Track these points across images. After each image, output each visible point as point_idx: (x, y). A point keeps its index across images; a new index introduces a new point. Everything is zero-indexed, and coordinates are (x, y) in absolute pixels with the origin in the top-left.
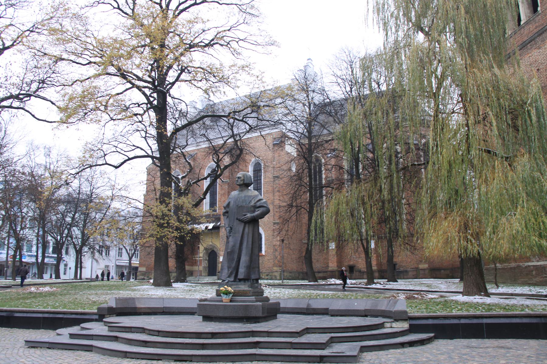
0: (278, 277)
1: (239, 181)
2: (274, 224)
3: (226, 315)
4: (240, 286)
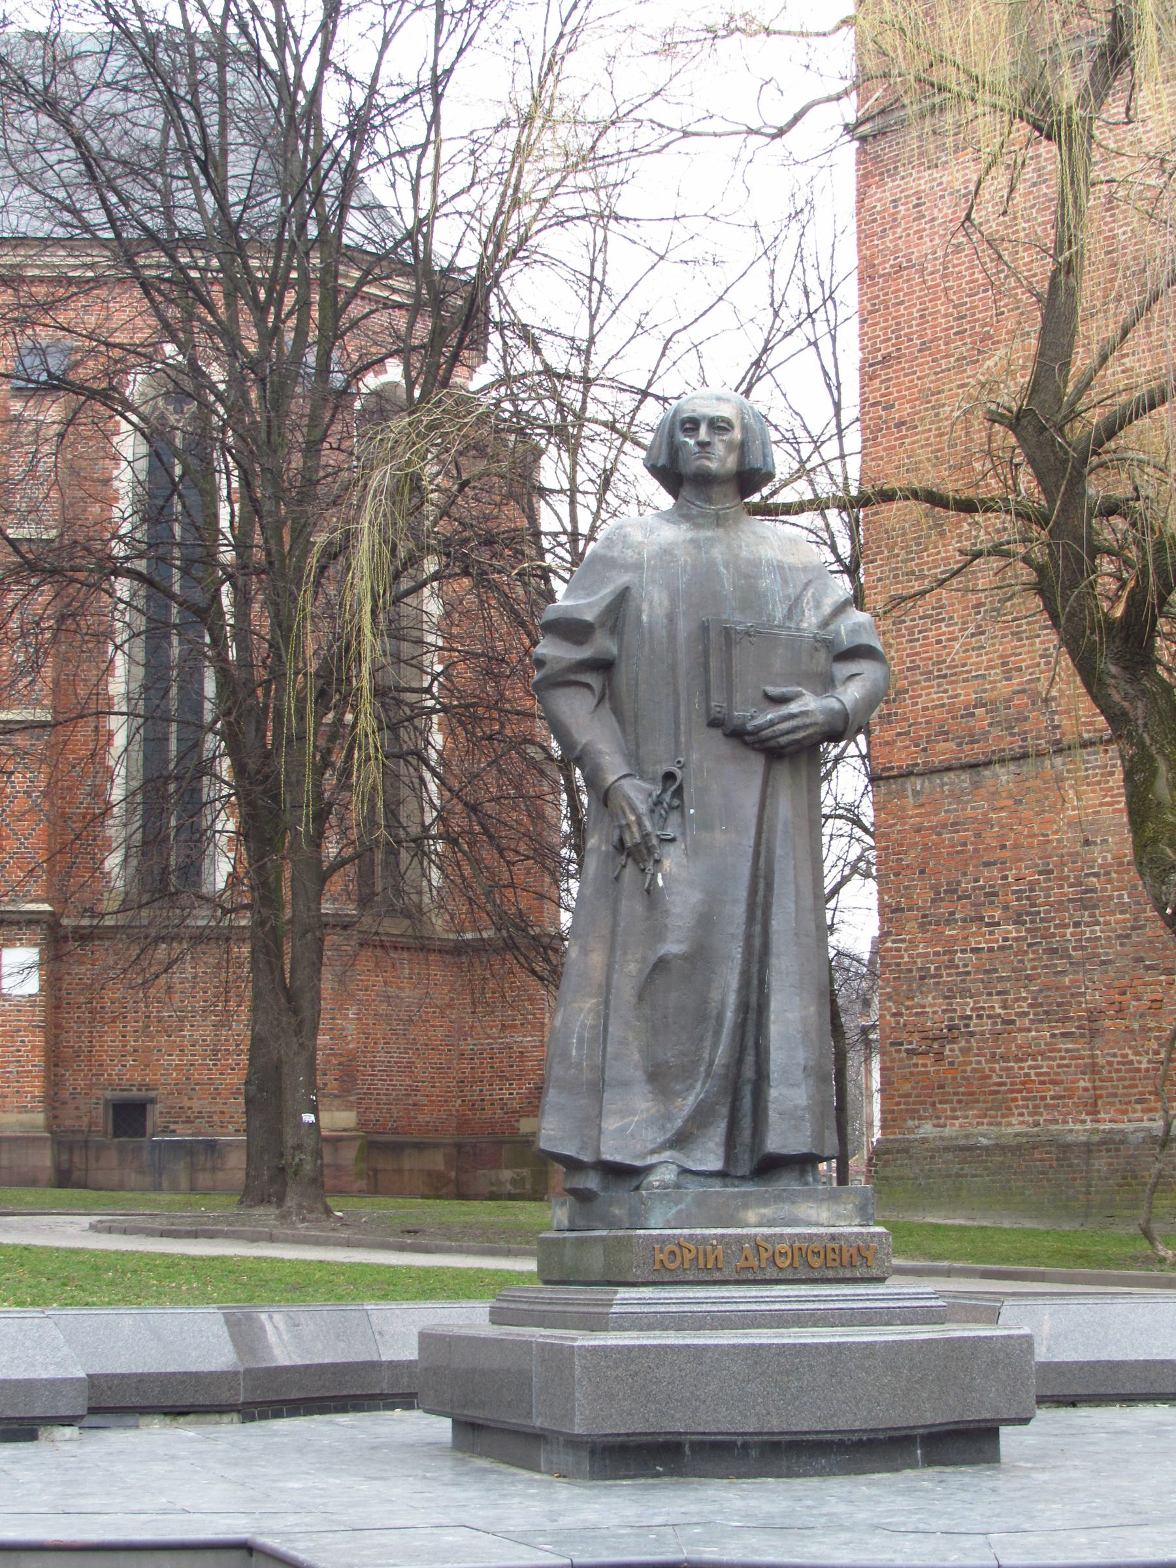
1: (719, 448)
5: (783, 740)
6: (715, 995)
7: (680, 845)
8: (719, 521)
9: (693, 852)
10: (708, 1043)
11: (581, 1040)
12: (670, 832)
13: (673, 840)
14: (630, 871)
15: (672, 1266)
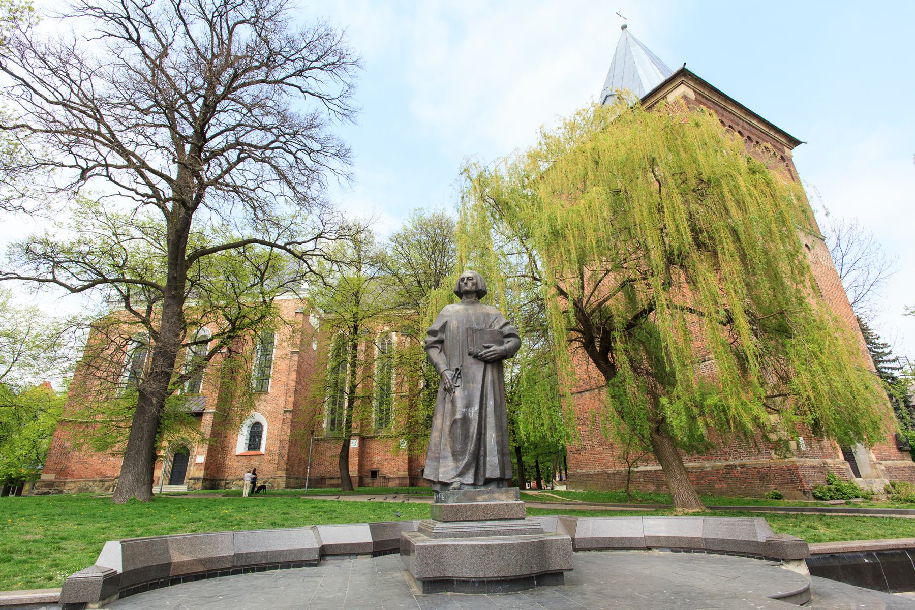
2: (285, 412)
3: (491, 574)
4: (496, 495)
6: (471, 430)
8: (473, 303)
9: (464, 389)
14: (448, 395)
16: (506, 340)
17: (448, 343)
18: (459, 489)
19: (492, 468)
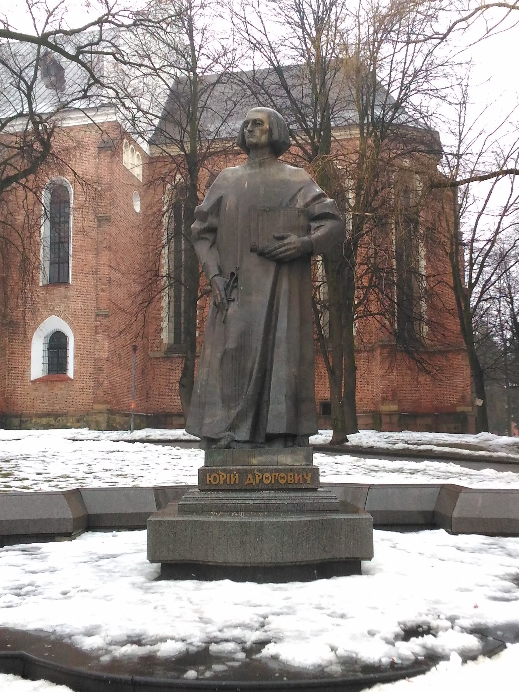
0: (104, 425)
1: (257, 133)
5: (281, 256)
6: (249, 365)
7: (236, 303)
10: (246, 386)
11: (201, 385)
12: (233, 297)
13: (234, 300)
15: (214, 483)
16: (314, 225)
17: (222, 232)
18: (228, 447)
19: (277, 421)
